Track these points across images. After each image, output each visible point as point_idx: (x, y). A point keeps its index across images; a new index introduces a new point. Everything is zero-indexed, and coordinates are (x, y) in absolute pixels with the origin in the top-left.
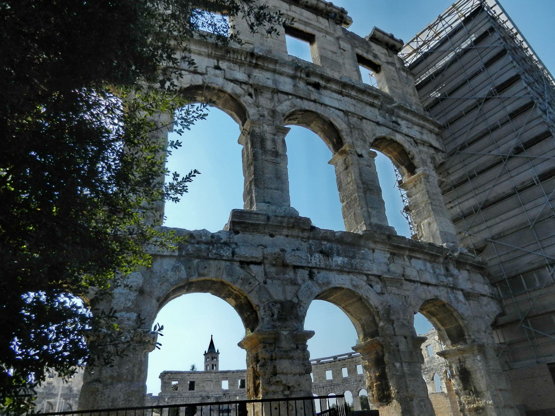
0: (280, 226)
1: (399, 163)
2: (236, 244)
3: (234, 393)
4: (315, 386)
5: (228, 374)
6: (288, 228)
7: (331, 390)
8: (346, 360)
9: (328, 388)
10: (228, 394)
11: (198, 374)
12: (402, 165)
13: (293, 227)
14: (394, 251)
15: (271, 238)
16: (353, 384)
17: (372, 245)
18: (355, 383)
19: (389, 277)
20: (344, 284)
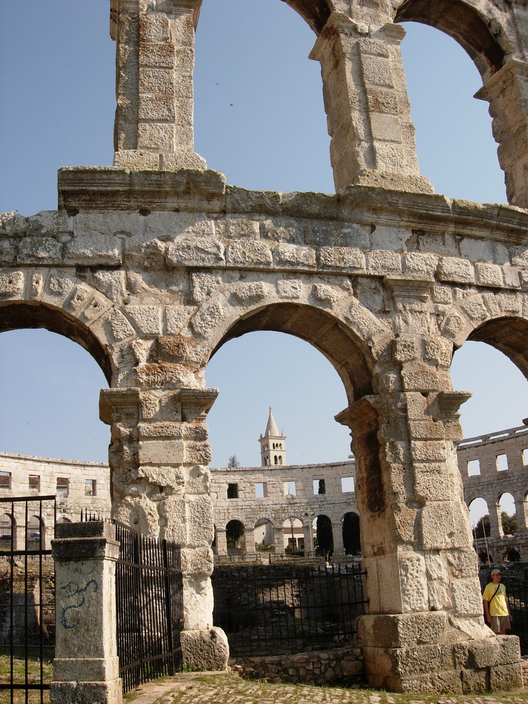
0: (159, 192)
1: (475, 47)
2: (71, 234)
5: (294, 471)
6: (177, 194)
7: (477, 492)
8: (505, 442)
9: (473, 489)
10: (296, 503)
12: (480, 51)
13: (187, 192)
14: (420, 226)
15: (142, 217)
16: (516, 481)
17: (369, 217)
18: (520, 480)
19: (399, 278)
20: (297, 298)
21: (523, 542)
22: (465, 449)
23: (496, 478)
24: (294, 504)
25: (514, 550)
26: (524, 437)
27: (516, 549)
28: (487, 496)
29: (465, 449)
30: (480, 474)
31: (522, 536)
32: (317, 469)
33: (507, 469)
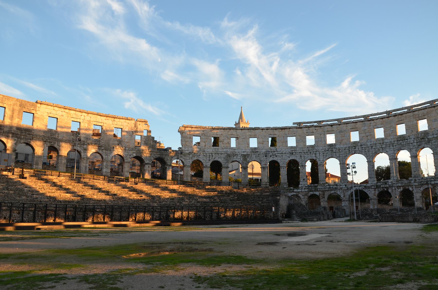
3: (264, 151)
4: (361, 146)
5: (257, 131)
8: (404, 115)
10: (257, 152)
11: (223, 130)
21: (416, 184)
22: (373, 120)
23: (396, 140)
24: (255, 152)
25: (408, 189)
26: (420, 111)
27: (411, 189)
28: (389, 152)
29: (373, 120)
30: (384, 137)
31: (415, 180)
32: (272, 131)
33: (405, 133)
